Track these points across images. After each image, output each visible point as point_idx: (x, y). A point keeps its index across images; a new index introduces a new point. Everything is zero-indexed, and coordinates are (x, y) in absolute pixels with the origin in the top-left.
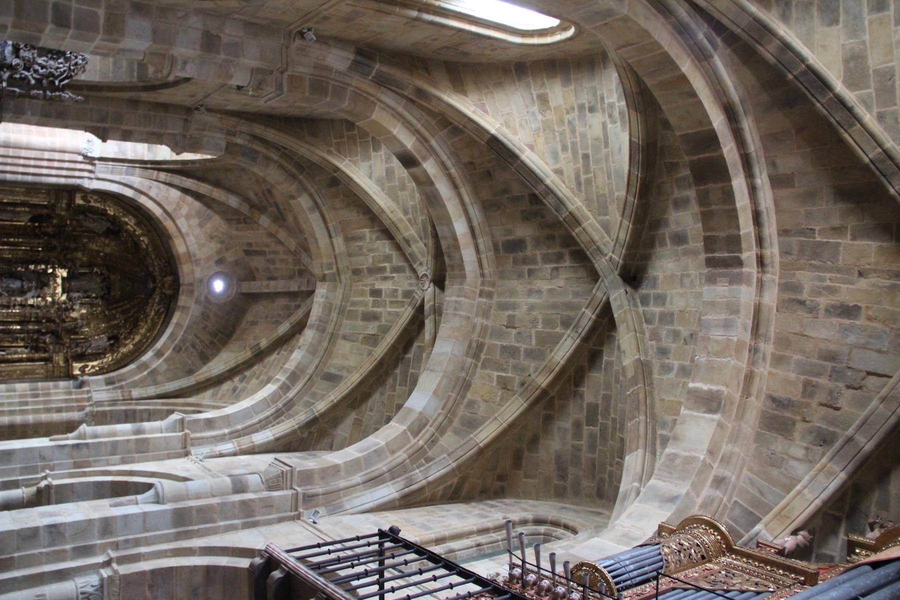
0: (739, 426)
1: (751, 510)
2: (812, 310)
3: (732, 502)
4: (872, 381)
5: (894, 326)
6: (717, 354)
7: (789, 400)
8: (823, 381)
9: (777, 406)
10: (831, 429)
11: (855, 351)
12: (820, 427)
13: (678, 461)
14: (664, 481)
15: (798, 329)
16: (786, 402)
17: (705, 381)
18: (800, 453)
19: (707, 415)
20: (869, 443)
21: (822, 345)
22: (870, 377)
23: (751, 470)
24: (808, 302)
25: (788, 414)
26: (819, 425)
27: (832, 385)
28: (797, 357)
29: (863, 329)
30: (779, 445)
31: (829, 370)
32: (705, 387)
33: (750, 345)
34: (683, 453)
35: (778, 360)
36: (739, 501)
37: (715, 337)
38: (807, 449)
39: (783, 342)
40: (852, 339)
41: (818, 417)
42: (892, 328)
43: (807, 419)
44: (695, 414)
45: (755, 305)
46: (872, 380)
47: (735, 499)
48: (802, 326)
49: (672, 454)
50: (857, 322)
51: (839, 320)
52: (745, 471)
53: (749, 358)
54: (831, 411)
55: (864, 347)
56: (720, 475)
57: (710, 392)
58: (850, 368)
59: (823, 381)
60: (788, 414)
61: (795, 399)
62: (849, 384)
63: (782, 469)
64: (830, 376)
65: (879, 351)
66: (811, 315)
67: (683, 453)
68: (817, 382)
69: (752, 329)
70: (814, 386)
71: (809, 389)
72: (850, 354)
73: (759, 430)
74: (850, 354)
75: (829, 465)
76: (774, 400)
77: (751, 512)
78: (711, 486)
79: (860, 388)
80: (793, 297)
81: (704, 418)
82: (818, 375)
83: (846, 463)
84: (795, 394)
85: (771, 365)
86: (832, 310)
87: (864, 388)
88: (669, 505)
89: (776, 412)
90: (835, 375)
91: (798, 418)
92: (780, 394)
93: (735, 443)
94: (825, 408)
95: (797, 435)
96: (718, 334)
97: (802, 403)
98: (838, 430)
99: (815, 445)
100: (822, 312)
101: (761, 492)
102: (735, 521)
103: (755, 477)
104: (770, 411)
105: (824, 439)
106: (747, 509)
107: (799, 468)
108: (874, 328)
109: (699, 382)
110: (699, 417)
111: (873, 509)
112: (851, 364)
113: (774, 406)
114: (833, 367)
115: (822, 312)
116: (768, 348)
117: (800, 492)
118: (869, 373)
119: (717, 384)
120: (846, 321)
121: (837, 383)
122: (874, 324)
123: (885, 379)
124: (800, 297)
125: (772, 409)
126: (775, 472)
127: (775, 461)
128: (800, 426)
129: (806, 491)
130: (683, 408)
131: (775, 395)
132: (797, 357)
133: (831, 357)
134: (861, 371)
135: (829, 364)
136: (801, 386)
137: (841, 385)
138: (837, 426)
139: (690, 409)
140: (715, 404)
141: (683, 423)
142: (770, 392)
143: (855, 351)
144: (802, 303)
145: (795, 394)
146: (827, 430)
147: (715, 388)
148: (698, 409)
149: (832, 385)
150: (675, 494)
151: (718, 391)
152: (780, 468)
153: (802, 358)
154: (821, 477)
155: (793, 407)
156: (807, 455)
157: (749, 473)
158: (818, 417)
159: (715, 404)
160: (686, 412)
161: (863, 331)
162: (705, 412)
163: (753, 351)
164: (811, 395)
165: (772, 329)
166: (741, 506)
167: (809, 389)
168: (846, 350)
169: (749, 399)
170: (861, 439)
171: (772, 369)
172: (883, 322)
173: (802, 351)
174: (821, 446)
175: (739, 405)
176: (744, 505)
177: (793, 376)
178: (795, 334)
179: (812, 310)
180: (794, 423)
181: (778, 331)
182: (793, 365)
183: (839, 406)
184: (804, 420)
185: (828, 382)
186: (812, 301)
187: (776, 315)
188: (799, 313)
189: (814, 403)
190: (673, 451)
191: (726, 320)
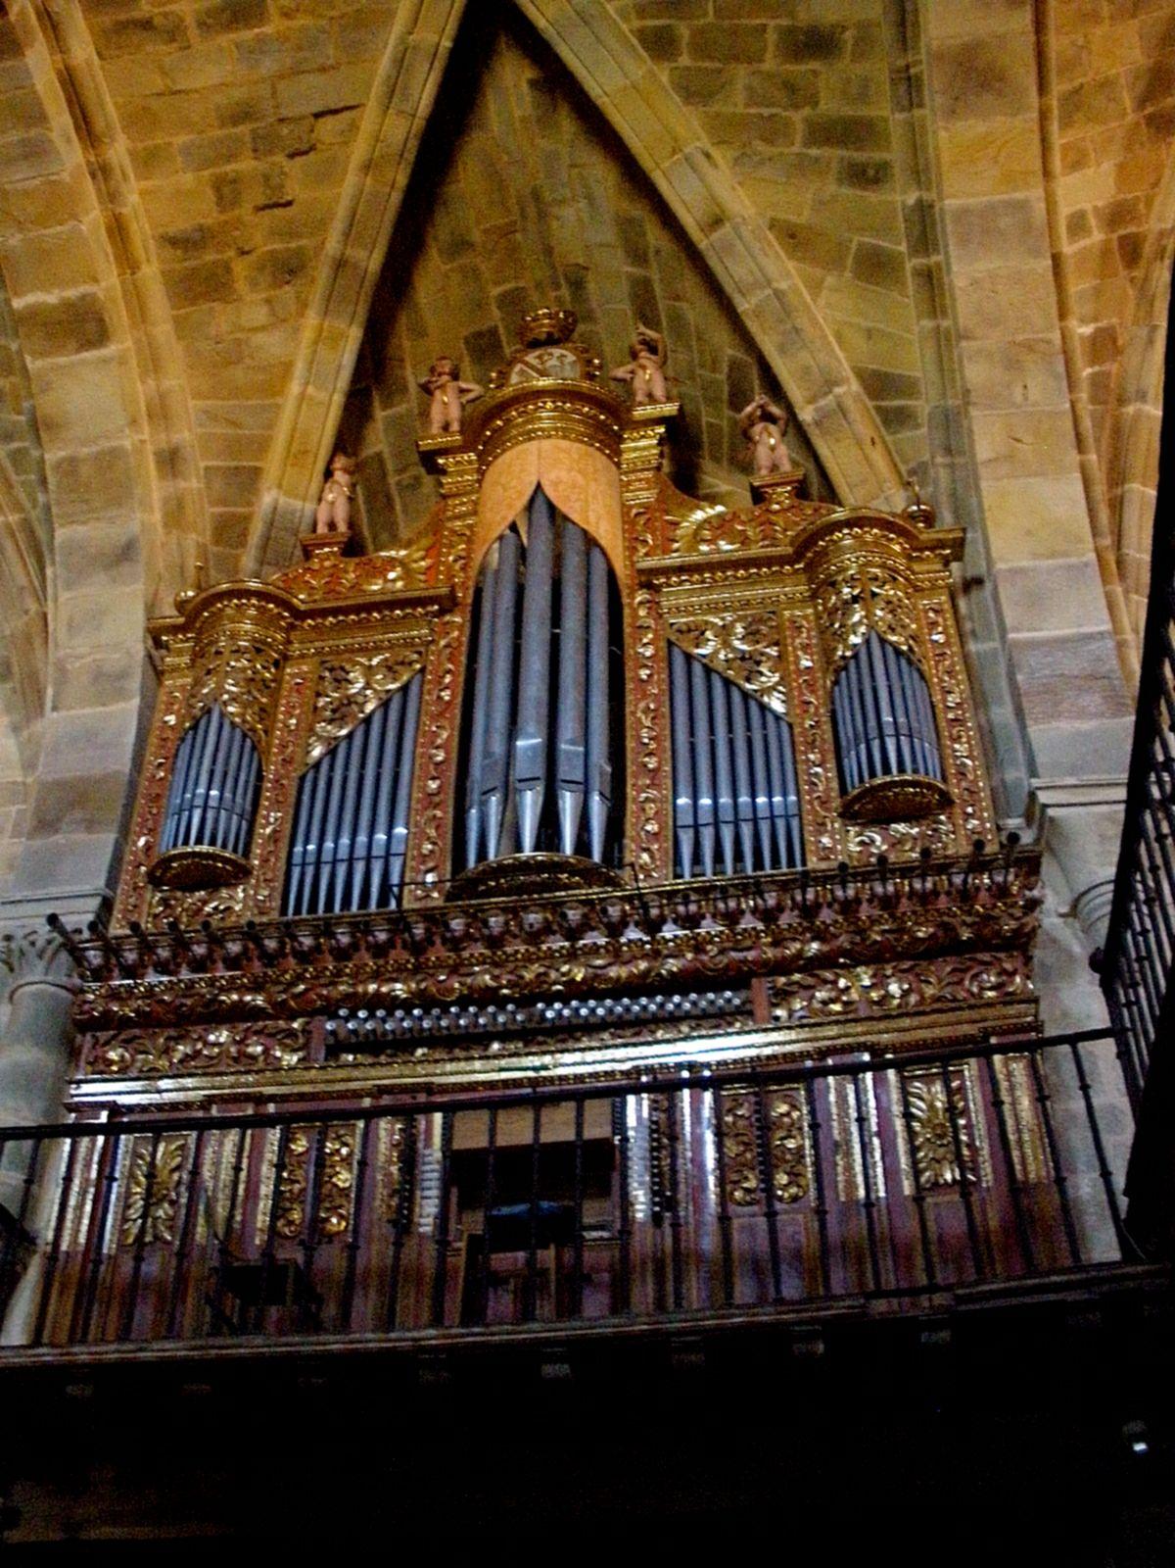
0: (146, 334)
1: (234, 464)
2: (174, 33)
3: (202, 472)
4: (328, 127)
5: (333, 13)
6: (42, 220)
7: (201, 228)
8: (246, 165)
9: (186, 250)
10: (293, 245)
11: (281, 86)
12: (272, 252)
13: (85, 470)
14: (84, 523)
15: (159, 83)
16: (197, 236)
17: (44, 287)
18: (260, 315)
19: (86, 355)
20: (375, 255)
21: (219, 99)
22: (322, 120)
23: (198, 395)
24: (156, 21)
25: (210, 257)
26: (269, 247)
27: (260, 166)
28: (181, 139)
29: (283, 38)
30: (221, 319)
31: (248, 139)
32: (51, 298)
33: (89, 163)
34: (85, 450)
35: (148, 161)
36: (210, 464)
37: (19, 186)
38: (268, 301)
39: (140, 119)
40: (268, 66)
41: (261, 235)
42: (332, 18)
43: (246, 249)
44: (62, 360)
45: (59, 73)
46: (328, 124)
47: (202, 465)
48: (164, 73)
49: (64, 459)
50: (268, 29)
51: (232, 36)
52: (191, 403)
53: (99, 190)
54: (277, 211)
55: (296, 71)
56: (164, 445)
57: (68, 305)
58: (281, 120)
59: (246, 165)
60: (210, 257)
61: (210, 221)
62: (292, 150)
63: (247, 361)
64: (255, 150)
65: (323, 69)
66: (175, 45)
67: (85, 450)
68: (236, 172)
69: (77, 128)
70: (234, 181)
71: (226, 191)
72: (274, 93)
73: (175, 312)
74: (274, 93)
75: (326, 323)
76: (173, 242)
77: (236, 468)
78: (162, 476)
79: (312, 148)
80: (123, 17)
81: (83, 362)
82: (231, 157)
83: (351, 308)
84: (205, 211)
85: (139, 177)
86: (210, 21)
87: (319, 146)
88: (126, 568)
89: (186, 264)
90: (262, 145)
91: (231, 253)
92: (180, 225)
93: (156, 372)
94: (268, 211)
95: (241, 286)
96: (19, 176)
97: (226, 222)
98: (304, 242)
99: (280, 287)
100: (193, 32)
101: (235, 424)
102: (224, 502)
103: (209, 402)
104: (177, 266)
105: (288, 269)
106: (229, 468)
107: (271, 344)
108: (304, 29)
109: (31, 291)
110: (73, 364)
111: (407, 344)
112: (285, 112)
113: (179, 252)
114: (253, 131)
115: (193, 32)
116: (119, 151)
117: (302, 396)
118: (318, 116)
119: (74, 283)
120: (247, 35)
121: (270, 159)
122: (302, 21)
123: (347, 115)
124: (136, 14)
125: (180, 262)
126: (238, 374)
127: (234, 354)
128: (240, 268)
129: (310, 389)
130: (28, 359)
131: (172, 231)
132: (181, 139)
133: (242, 114)
134: (302, 118)
135: (243, 130)
136: (210, 194)
137: (280, 158)
138: (300, 236)
139: (43, 354)
140: (91, 327)
141: (47, 388)
142: (161, 230)
143: (281, 86)
144: (147, 25)
145: (205, 211)
146: (288, 250)
147: (72, 293)
148: (60, 349)
149: (260, 166)
150: (124, 540)
151: (83, 297)
152: (239, 361)
153: (192, 137)
154: (324, 352)
155: (213, 237)
156: (273, 312)
157: (200, 403)
158: (261, 235)
159: (91, 327)
160: (39, 363)
161: (283, 43)
162: (78, 351)
163: (99, 173)
164: (235, 203)
165: (110, 108)
166: (218, 468)
167: (226, 190)
168: (264, 90)
169: (139, 275)
170: (358, 254)
171: (144, 184)
172: (312, 13)
173: (186, 125)
174: (288, 283)
175: (125, 292)
176: (221, 464)
177: (188, 179)
178: (158, 95)
179: (174, 33)
180: (228, 270)
181: (121, 100)
182: (180, 159)
183: (290, 198)
184: (243, 253)
185: (254, 163)
186: (165, 15)
187: (102, 68)
188: (149, 48)
189: (245, 211)
190: (63, 454)
191: (23, 142)
